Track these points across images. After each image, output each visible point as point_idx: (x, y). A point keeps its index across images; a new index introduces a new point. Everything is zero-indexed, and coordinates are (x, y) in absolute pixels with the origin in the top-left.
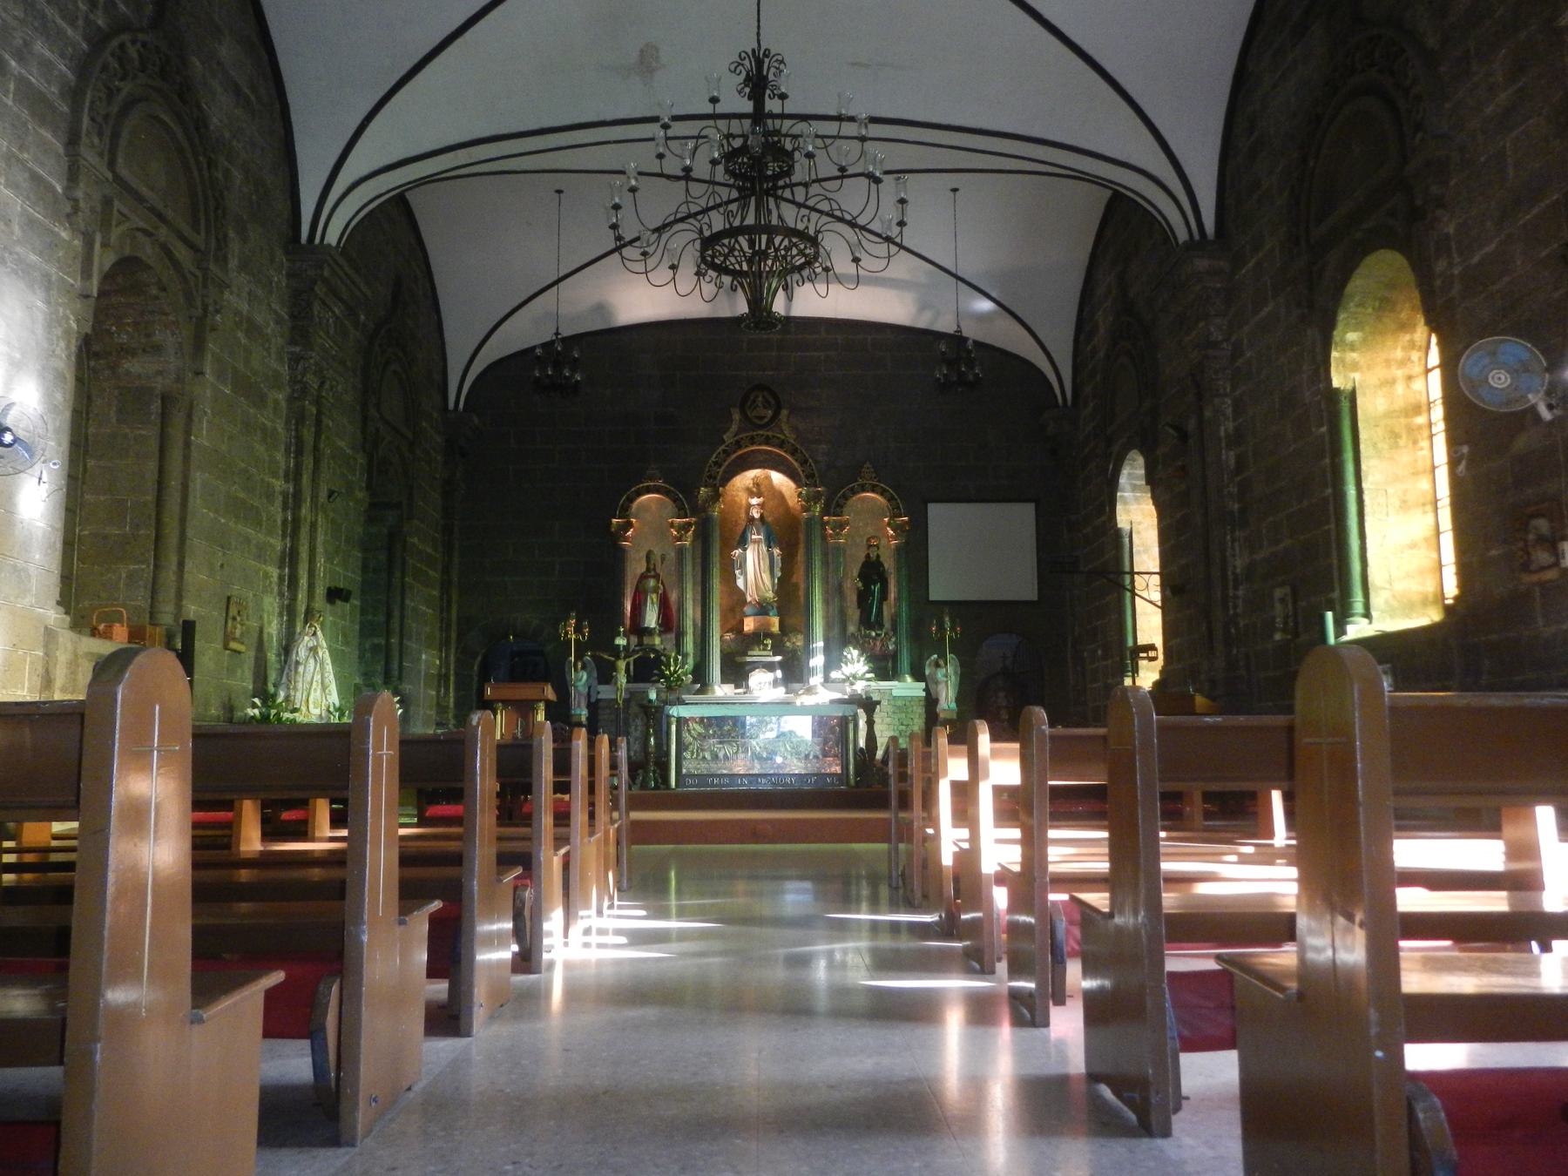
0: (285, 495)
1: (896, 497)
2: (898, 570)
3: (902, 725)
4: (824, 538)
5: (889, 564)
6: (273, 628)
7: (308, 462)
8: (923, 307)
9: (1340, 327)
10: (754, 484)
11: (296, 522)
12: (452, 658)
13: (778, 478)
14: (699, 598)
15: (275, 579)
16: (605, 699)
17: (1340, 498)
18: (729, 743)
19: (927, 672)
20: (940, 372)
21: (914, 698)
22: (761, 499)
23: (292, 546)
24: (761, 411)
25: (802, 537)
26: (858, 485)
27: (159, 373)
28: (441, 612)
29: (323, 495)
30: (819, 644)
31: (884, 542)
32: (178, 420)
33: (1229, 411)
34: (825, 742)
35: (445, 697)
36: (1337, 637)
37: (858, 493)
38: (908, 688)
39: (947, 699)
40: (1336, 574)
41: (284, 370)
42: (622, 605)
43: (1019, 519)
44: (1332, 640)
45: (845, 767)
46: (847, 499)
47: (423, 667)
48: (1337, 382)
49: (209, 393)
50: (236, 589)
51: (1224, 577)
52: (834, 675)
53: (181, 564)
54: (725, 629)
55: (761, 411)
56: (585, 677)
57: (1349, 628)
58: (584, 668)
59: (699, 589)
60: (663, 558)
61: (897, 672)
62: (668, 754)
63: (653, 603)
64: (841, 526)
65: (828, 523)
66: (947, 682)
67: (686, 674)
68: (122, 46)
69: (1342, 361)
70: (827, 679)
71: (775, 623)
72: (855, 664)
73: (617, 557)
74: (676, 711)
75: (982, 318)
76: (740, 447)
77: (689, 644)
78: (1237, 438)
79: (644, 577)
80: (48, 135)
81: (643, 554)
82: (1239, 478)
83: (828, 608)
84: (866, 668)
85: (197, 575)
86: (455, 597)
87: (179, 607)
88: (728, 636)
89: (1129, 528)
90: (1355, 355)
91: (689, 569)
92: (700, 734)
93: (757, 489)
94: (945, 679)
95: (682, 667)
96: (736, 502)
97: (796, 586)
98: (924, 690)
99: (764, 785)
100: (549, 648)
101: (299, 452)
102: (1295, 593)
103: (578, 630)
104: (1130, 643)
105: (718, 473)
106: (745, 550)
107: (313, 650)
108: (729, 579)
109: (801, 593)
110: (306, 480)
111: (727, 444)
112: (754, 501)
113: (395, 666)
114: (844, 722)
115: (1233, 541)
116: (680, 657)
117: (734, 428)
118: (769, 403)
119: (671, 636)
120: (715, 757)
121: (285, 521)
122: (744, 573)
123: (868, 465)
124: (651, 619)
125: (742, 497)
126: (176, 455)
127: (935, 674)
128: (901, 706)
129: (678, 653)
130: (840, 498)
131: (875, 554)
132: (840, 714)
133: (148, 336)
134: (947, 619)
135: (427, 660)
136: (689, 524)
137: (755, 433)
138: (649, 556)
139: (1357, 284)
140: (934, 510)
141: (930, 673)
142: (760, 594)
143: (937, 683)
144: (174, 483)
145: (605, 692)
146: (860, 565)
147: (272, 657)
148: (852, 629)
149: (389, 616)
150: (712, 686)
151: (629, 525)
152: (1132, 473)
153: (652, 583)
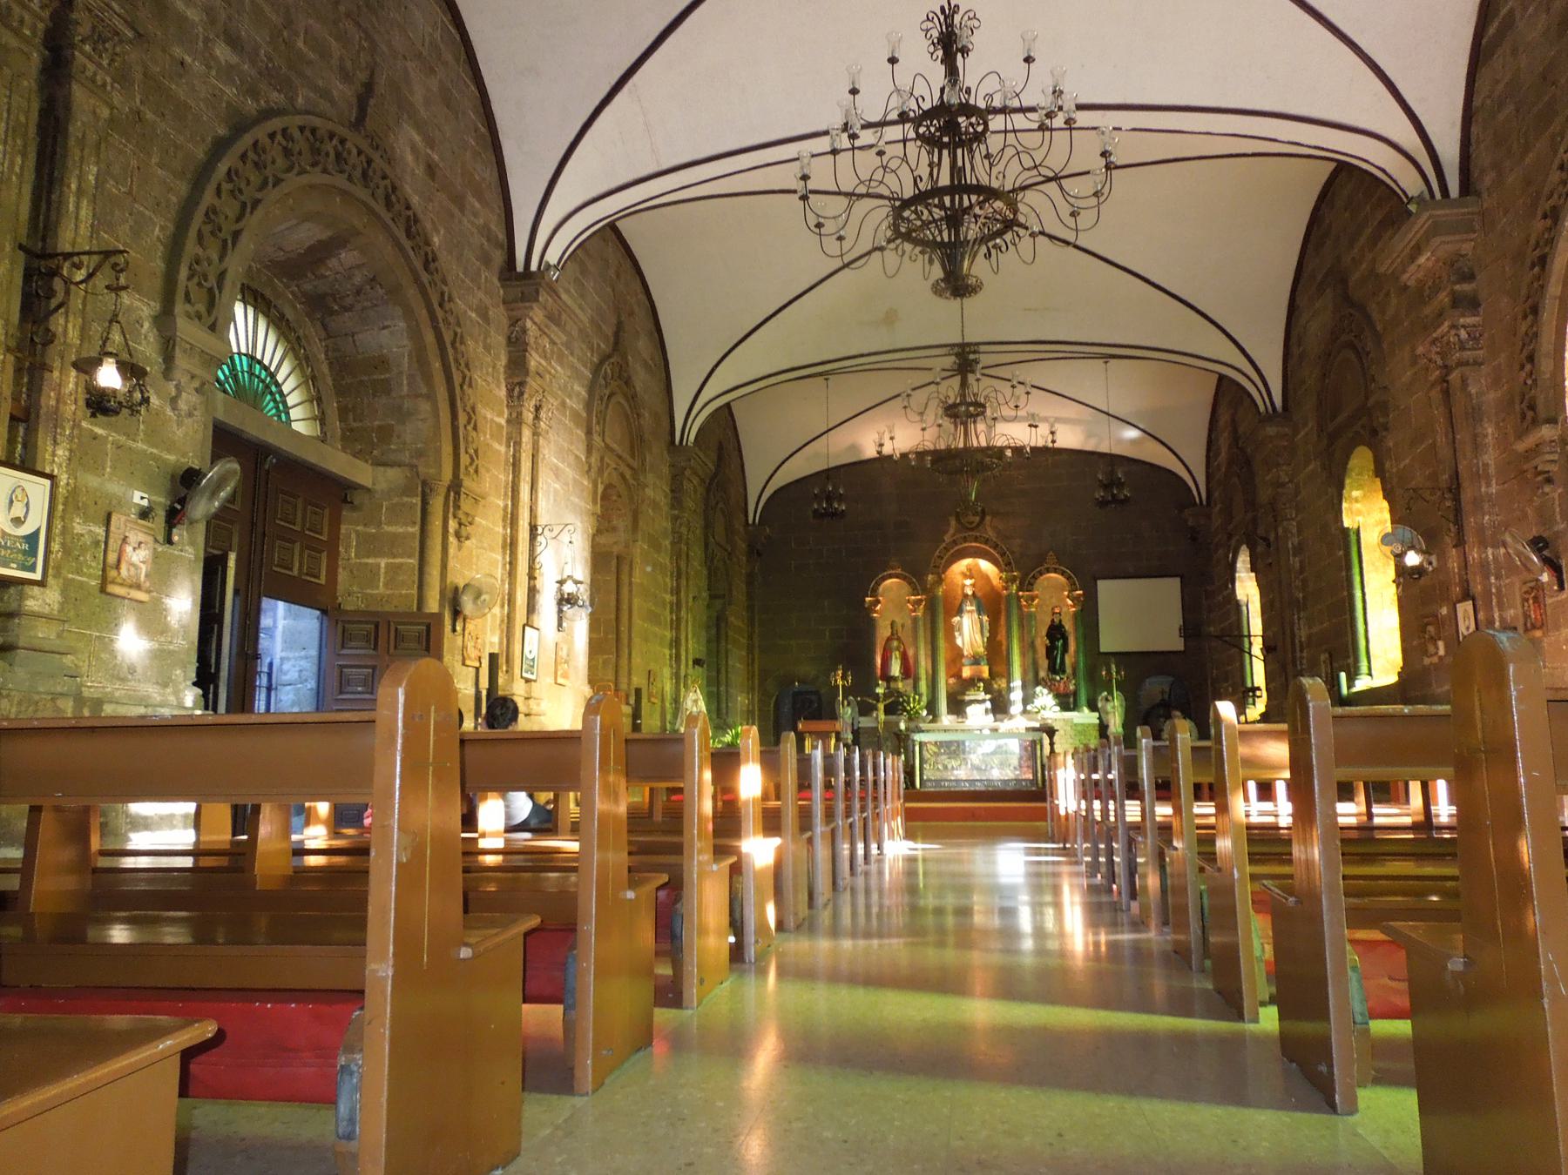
0: (671, 604)
2: (1076, 630)
4: (1020, 607)
5: (1068, 626)
6: (668, 688)
7: (684, 582)
8: (1089, 435)
9: (1347, 487)
11: (679, 619)
12: (756, 699)
13: (986, 566)
14: (930, 653)
15: (668, 657)
17: (1351, 597)
18: (955, 758)
19: (1100, 705)
20: (1099, 494)
23: (677, 638)
24: (972, 518)
25: (1003, 607)
27: (615, 543)
29: (691, 600)
30: (1017, 683)
31: (1064, 609)
32: (626, 569)
33: (1295, 530)
34: (1021, 758)
36: (1349, 687)
38: (1086, 717)
39: (1116, 724)
40: (1350, 646)
41: (668, 525)
42: (874, 659)
43: (1168, 591)
44: (1345, 691)
45: (1035, 774)
47: (739, 705)
48: (1347, 522)
49: (639, 551)
50: (652, 666)
51: (1293, 643)
52: (1029, 708)
53: (630, 654)
54: (949, 676)
55: (972, 518)
56: (850, 711)
57: (1357, 682)
58: (849, 704)
59: (930, 647)
60: (903, 626)
62: (913, 767)
64: (1033, 600)
65: (1022, 597)
67: (921, 709)
68: (606, 372)
69: (1350, 509)
70: (1025, 712)
71: (985, 671)
72: (1045, 700)
73: (869, 626)
74: (918, 737)
75: (1133, 442)
76: (956, 544)
77: (923, 686)
78: (1299, 550)
79: (889, 640)
80: (579, 432)
81: (888, 623)
82: (1301, 577)
84: (1054, 703)
85: (637, 660)
86: (756, 656)
87: (630, 679)
88: (952, 681)
89: (1245, 600)
90: (1358, 506)
91: (921, 633)
92: (935, 753)
93: (969, 574)
95: (919, 704)
97: (1000, 644)
99: (979, 787)
100: (823, 691)
101: (679, 577)
102: (1331, 656)
103: (844, 678)
104: (1249, 685)
106: (961, 617)
107: (696, 701)
108: (950, 638)
109: (1004, 648)
110: (682, 594)
112: (968, 582)
113: (724, 706)
114: (1033, 743)
115: (1299, 619)
116: (917, 697)
117: (952, 531)
119: (910, 681)
120: (945, 767)
121: (672, 619)
122: (961, 634)
123: (1051, 553)
124: (896, 670)
125: (959, 579)
126: (625, 591)
128: (1081, 730)
129: (916, 693)
132: (1031, 739)
133: (609, 522)
134: (1113, 666)
135: (741, 700)
136: (921, 600)
138: (893, 624)
139: (1354, 462)
140: (1101, 584)
144: (625, 607)
145: (865, 722)
147: (668, 705)
148: (1042, 674)
149: (718, 672)
151: (878, 602)
152: (1243, 561)
153: (895, 643)
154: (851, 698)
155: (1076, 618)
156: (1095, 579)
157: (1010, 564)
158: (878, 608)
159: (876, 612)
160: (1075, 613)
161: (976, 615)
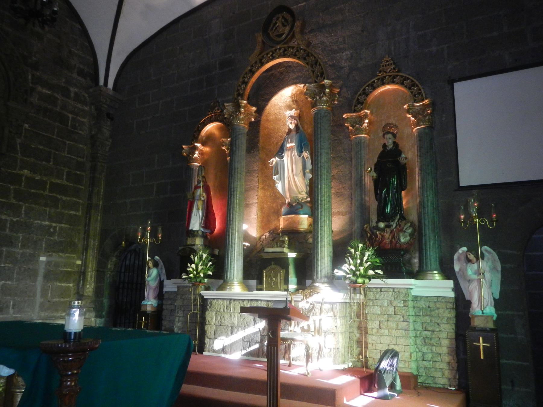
1: (417, 83)
3: (426, 330)
10: (293, 101)
16: (168, 292)
19: (457, 268)
21: (440, 300)
22: (293, 112)
26: (378, 79)
28: (85, 227)
35: (82, 287)
37: (379, 86)
46: (367, 95)
61: (423, 267)
63: (198, 209)
64: (361, 122)
66: (479, 281)
76: (262, 64)
83: (352, 204)
94: (475, 277)
96: (279, 120)
98: (453, 290)
103: (154, 234)
105: (245, 89)
111: (251, 64)
112: (289, 113)
118: (286, 20)
127: (466, 270)
130: (360, 95)
131: (391, 142)
137: (274, 49)
141: (460, 270)
142: (293, 195)
143: (470, 281)
146: (378, 156)
150: (233, 282)
154: (157, 258)
155: (420, 140)
156: (451, 83)
157: (322, 74)
158: (196, 155)
159: (195, 160)
160: (420, 134)
161: (295, 153)
